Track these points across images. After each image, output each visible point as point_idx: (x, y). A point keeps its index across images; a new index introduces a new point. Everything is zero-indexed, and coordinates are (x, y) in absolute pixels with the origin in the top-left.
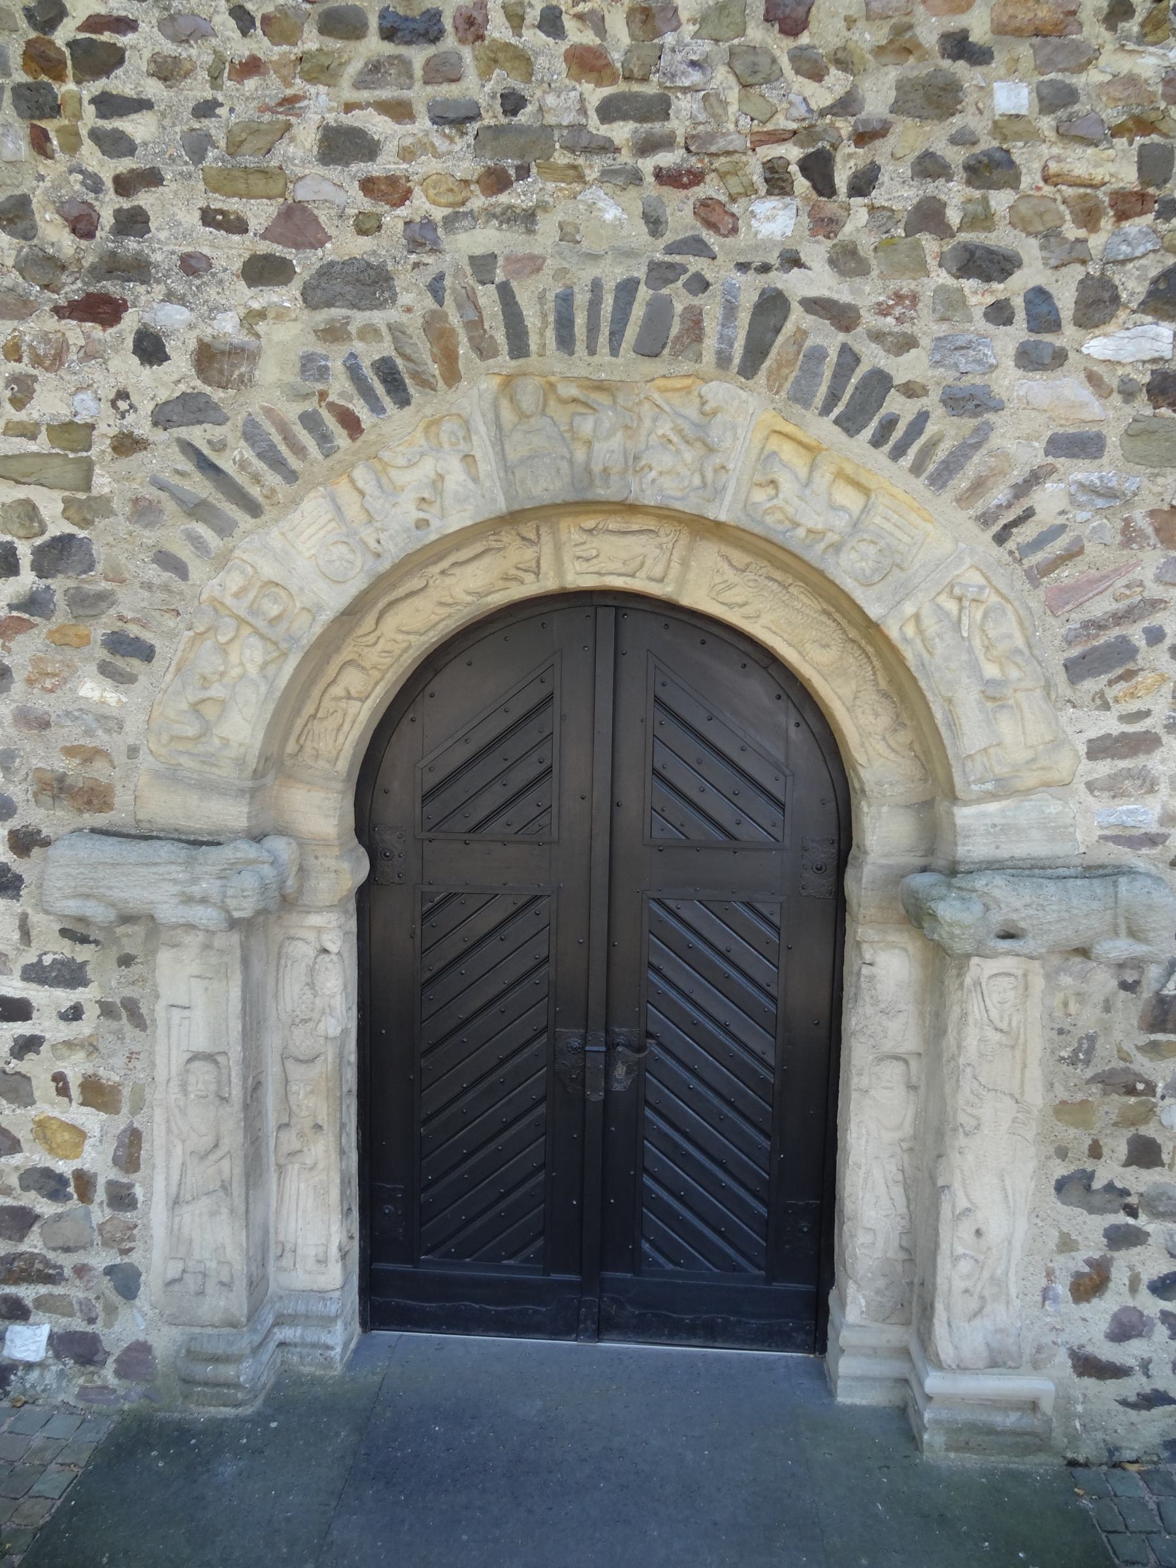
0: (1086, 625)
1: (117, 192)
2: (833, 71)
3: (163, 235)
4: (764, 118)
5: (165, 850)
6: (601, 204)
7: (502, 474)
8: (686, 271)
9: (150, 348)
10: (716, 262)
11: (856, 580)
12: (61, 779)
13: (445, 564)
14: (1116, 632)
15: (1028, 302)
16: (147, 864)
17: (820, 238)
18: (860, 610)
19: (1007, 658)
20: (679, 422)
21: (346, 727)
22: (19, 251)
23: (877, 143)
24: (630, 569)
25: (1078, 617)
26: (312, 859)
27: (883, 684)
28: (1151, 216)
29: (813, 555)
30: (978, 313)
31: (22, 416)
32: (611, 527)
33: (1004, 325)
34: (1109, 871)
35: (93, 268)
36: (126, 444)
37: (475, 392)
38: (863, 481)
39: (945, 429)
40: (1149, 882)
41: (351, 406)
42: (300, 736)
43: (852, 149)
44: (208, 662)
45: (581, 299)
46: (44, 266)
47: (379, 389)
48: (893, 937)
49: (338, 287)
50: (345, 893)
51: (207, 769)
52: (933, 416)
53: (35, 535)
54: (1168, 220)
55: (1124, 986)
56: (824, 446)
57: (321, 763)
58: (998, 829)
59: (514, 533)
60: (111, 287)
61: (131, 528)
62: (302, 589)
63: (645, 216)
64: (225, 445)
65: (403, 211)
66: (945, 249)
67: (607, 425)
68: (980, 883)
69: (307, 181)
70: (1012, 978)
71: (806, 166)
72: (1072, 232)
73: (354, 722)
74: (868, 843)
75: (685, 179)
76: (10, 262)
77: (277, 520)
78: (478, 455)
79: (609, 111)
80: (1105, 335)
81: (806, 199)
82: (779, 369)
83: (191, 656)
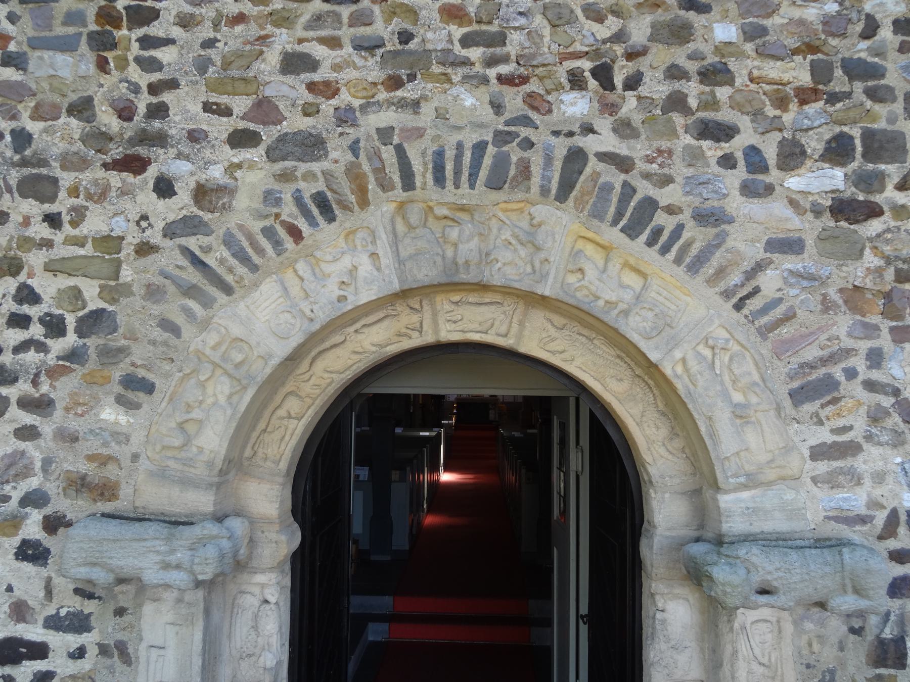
0: (802, 366)
1: (149, 93)
2: (610, 17)
3: (177, 119)
4: (567, 45)
5: (152, 529)
6: (462, 96)
7: (397, 265)
8: (518, 136)
9: (164, 188)
10: (538, 131)
11: (640, 334)
12: (83, 478)
13: (358, 325)
14: (823, 371)
15: (746, 155)
16: (139, 540)
17: (606, 115)
18: (646, 357)
19: (748, 388)
20: (516, 230)
21: (287, 438)
22: (83, 130)
23: (641, 59)
24: (484, 328)
25: (796, 361)
26: (260, 533)
27: (661, 406)
28: (822, 102)
29: (611, 318)
30: (713, 162)
31: (76, 232)
32: (470, 300)
33: (731, 169)
34: (833, 542)
35: (130, 139)
36: (145, 249)
37: (379, 213)
38: (642, 269)
39: (696, 235)
40: (865, 552)
41: (296, 223)
42: (254, 444)
43: (625, 62)
44: (191, 393)
45: (450, 154)
47: (315, 211)
48: (678, 590)
49: (290, 148)
50: (282, 558)
51: (187, 469)
52: (687, 227)
53: (79, 310)
54: (833, 105)
55: (853, 631)
56: (615, 246)
57: (269, 464)
58: (751, 510)
59: (405, 304)
60: (142, 151)
61: (144, 304)
62: (258, 343)
63: (491, 103)
64: (211, 249)
65: (334, 102)
66: (688, 122)
67: (468, 233)
68: (742, 552)
69: (272, 84)
70: (769, 624)
71: (595, 73)
72: (771, 112)
73: (292, 435)
74: (656, 520)
75: (517, 81)
76: (77, 136)
77: (243, 297)
78: (381, 253)
79: (466, 41)
80: (799, 175)
81: (596, 92)
82: (582, 197)
83: (180, 390)
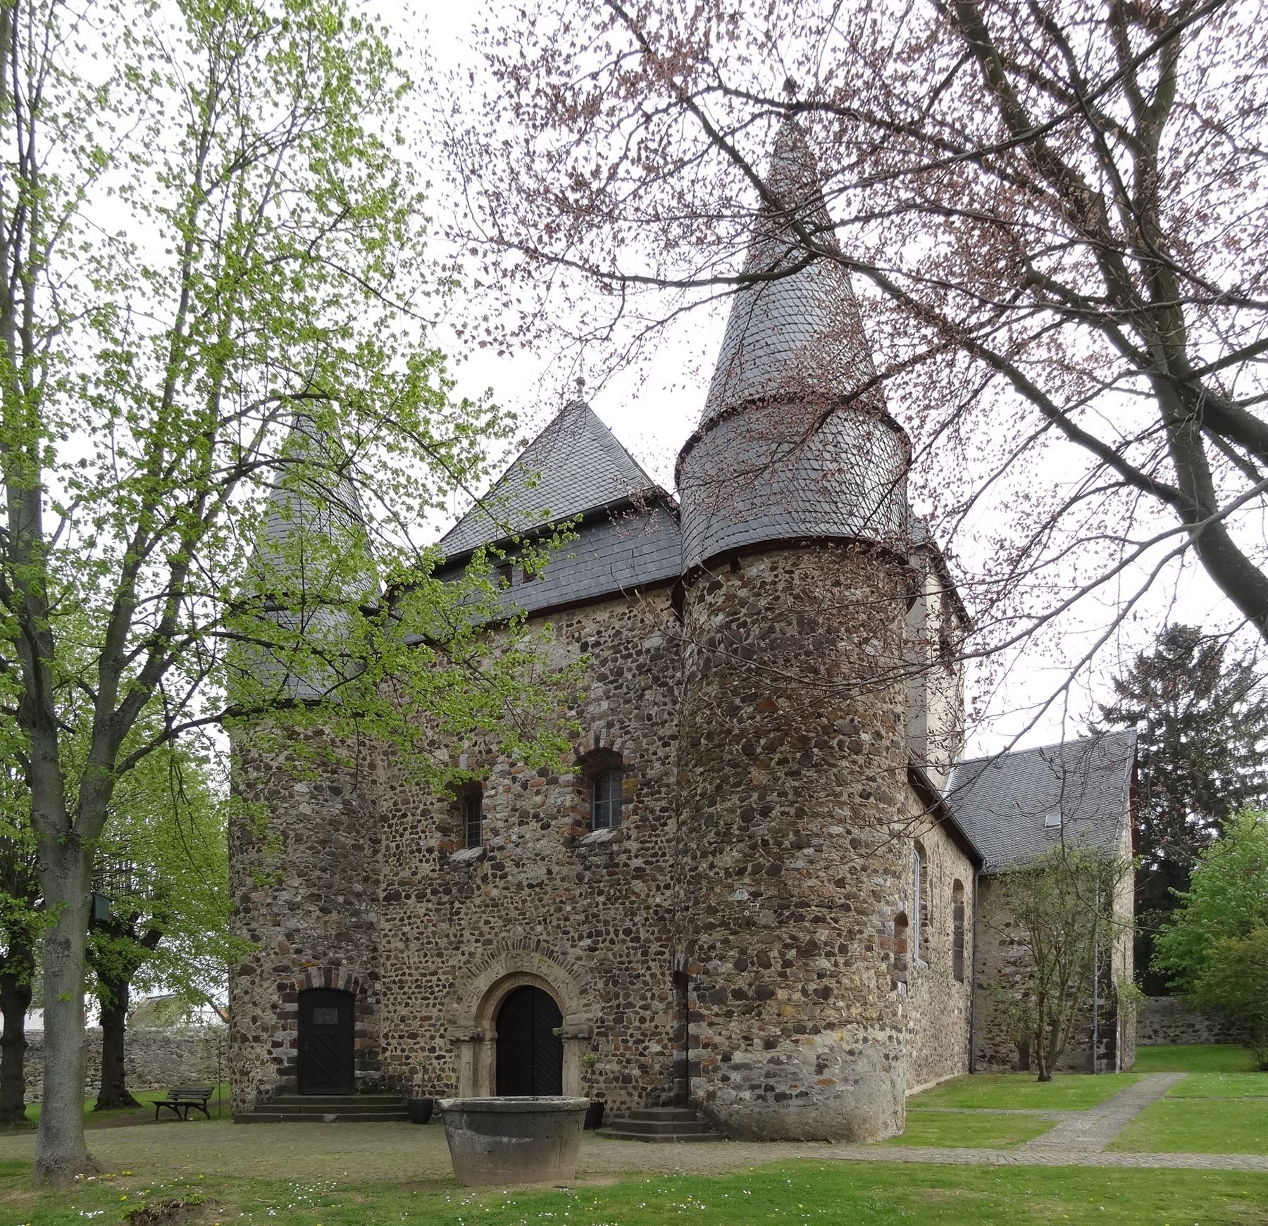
46: (451, 943)
